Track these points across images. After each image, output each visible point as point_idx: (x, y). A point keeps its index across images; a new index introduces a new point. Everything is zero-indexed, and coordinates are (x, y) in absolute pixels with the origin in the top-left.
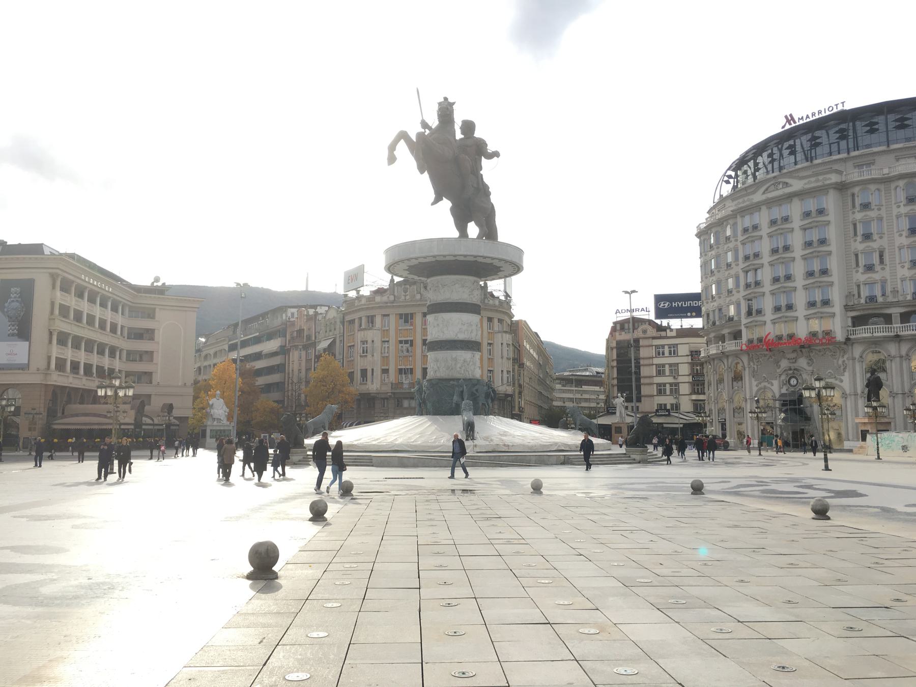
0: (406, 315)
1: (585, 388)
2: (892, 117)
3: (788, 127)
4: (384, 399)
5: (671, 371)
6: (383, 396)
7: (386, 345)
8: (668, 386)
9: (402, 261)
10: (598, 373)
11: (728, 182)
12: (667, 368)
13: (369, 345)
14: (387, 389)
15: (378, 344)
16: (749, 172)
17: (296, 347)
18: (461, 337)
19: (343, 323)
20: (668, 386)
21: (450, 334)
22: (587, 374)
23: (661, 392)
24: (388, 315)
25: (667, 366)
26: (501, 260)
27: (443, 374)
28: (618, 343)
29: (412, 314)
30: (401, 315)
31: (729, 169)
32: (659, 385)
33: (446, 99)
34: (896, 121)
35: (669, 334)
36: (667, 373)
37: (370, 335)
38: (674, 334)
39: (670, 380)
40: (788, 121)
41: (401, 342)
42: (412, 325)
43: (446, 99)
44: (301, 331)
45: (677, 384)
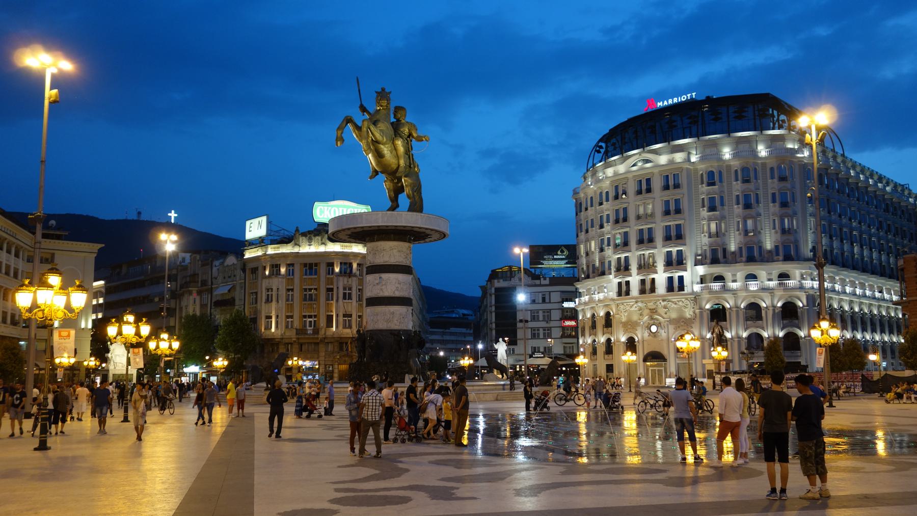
0: (311, 265)
1: (453, 330)
2: (732, 109)
3: (649, 110)
4: (288, 344)
5: (544, 316)
6: (287, 341)
7: (290, 293)
8: (541, 330)
9: (349, 229)
10: (464, 315)
11: (599, 152)
12: (541, 312)
13: (274, 293)
14: (291, 334)
15: (283, 292)
16: (617, 145)
17: (190, 293)
18: (397, 294)
19: (244, 270)
20: (541, 330)
21: (388, 292)
22: (454, 316)
23: (535, 336)
24: (293, 265)
25: (541, 312)
26: (432, 230)
27: (382, 325)
28: (497, 290)
29: (316, 265)
30: (305, 265)
31: (601, 140)
32: (533, 329)
33: (383, 90)
34: (735, 112)
35: (543, 282)
36: (541, 318)
37: (275, 283)
38: (547, 282)
39: (544, 324)
40: (649, 105)
41: (305, 290)
42: (316, 274)
43: (383, 90)
44: (195, 275)
45: (550, 329)
